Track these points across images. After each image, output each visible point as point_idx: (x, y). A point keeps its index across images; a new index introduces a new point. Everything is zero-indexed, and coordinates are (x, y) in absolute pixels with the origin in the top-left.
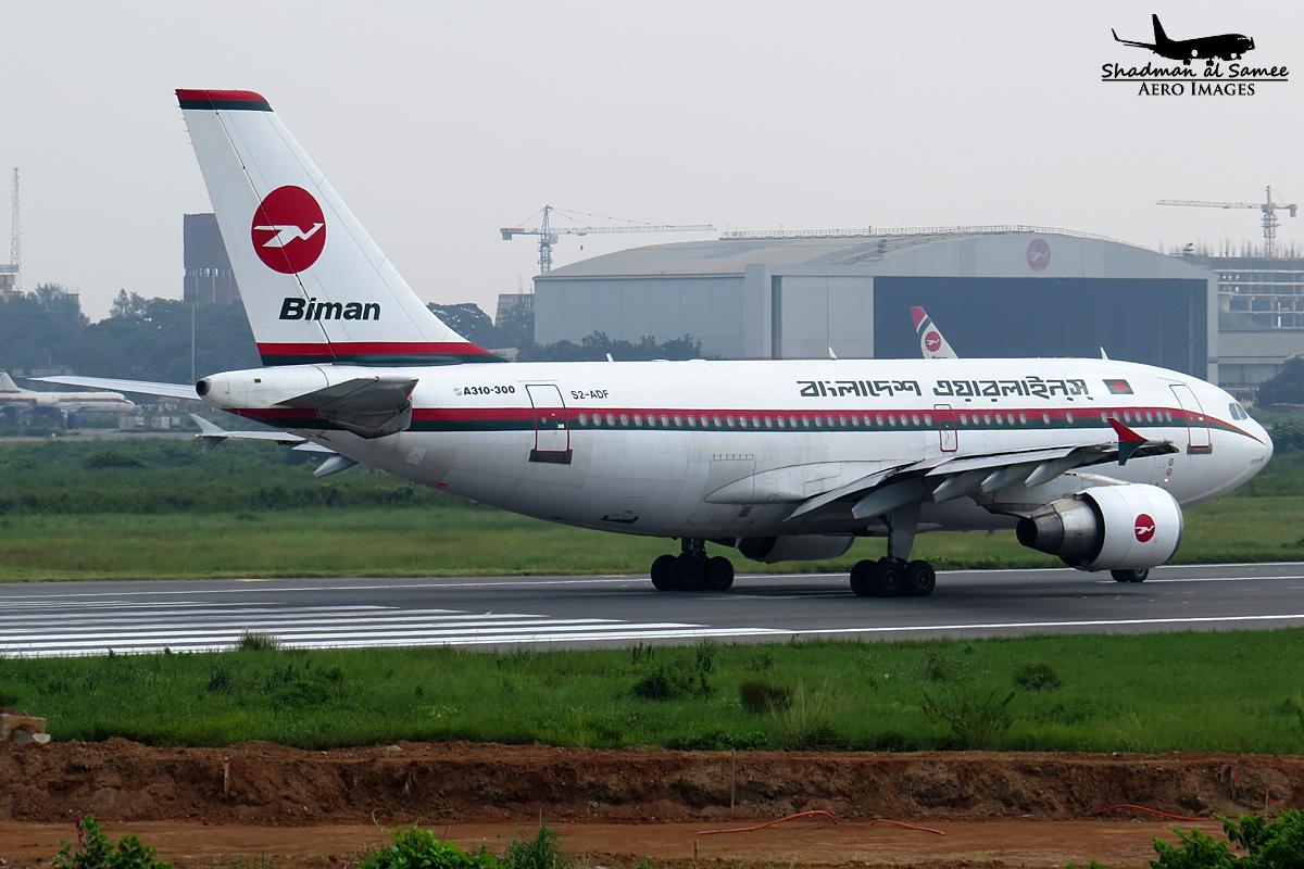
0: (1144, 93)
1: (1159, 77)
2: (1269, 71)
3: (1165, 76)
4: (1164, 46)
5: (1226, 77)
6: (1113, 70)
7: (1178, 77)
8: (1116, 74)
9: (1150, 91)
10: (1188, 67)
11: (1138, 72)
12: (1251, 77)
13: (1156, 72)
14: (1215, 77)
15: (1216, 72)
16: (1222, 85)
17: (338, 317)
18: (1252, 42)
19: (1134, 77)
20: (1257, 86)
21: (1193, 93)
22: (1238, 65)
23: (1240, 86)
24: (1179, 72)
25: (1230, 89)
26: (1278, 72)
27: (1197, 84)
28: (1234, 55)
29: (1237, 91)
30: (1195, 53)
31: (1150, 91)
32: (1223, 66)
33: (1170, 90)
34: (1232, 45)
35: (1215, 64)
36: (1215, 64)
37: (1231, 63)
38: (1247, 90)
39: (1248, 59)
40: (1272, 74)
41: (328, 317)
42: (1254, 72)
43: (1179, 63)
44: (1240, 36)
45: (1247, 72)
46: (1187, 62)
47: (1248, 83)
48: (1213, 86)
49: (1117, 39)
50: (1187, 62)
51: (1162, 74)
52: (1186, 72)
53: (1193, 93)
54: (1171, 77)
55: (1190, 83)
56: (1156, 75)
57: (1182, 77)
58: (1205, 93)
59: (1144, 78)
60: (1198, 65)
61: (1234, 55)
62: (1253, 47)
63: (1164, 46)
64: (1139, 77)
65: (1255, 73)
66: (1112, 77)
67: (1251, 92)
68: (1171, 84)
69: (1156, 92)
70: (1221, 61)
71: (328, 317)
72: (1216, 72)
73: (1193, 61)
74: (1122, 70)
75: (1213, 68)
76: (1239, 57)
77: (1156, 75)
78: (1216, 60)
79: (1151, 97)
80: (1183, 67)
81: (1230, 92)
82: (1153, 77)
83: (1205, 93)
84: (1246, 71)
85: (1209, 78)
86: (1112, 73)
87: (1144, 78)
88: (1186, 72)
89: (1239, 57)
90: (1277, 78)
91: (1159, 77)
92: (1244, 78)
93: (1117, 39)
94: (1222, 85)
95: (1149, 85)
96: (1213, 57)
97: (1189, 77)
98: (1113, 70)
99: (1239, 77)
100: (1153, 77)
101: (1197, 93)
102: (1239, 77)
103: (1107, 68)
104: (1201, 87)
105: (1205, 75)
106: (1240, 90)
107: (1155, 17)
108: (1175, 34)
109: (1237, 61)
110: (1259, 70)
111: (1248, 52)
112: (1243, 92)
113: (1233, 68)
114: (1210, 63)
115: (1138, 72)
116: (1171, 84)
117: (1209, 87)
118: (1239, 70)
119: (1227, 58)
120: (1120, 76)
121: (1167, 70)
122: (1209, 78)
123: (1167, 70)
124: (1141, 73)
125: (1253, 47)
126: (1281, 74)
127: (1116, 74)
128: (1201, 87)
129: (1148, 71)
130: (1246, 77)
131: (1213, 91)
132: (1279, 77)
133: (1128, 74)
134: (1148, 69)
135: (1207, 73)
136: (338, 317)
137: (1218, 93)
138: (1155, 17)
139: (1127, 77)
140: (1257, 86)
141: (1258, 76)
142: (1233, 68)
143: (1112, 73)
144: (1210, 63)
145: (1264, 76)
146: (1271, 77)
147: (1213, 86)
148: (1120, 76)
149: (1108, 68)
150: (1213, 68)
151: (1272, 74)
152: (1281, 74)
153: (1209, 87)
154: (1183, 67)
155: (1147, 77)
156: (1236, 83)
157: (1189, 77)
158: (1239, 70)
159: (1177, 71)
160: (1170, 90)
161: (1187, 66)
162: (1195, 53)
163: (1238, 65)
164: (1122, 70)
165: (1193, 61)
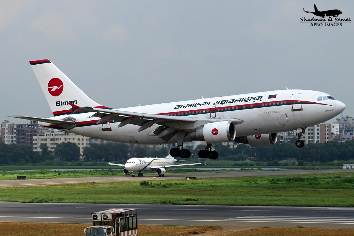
0: (312, 25)
1: (316, 21)
2: (346, 20)
3: (318, 21)
4: (317, 13)
5: (334, 21)
6: (303, 19)
7: (321, 21)
8: (304, 21)
9: (313, 25)
10: (324, 19)
12: (341, 21)
13: (315, 20)
14: (331, 21)
15: (331, 20)
16: (333, 23)
17: (67, 104)
18: (341, 12)
19: (309, 21)
20: (342, 24)
21: (325, 26)
22: (337, 18)
23: (338, 24)
24: (321, 20)
25: (335, 25)
26: (348, 20)
27: (326, 23)
28: (336, 15)
30: (325, 15)
31: (313, 25)
32: (333, 18)
33: (319, 25)
34: (335, 13)
35: (331, 18)
36: (331, 18)
38: (340, 25)
39: (340, 16)
40: (347, 20)
41: (65, 104)
42: (342, 20)
43: (321, 17)
46: (323, 17)
48: (331, 24)
49: (304, 11)
50: (323, 17)
51: (317, 20)
52: (323, 20)
53: (325, 26)
54: (319, 21)
55: (324, 23)
56: (315, 21)
57: (322, 21)
58: (328, 25)
60: (326, 18)
61: (336, 15)
62: (341, 13)
63: (317, 13)
64: (310, 21)
65: (342, 20)
66: (303, 21)
67: (341, 25)
68: (319, 23)
69: (315, 25)
70: (333, 17)
71: (65, 104)
72: (331, 20)
73: (325, 17)
74: (306, 19)
75: (331, 19)
76: (337, 16)
77: (315, 21)
78: (331, 17)
79: (314, 27)
80: (322, 19)
81: (335, 25)
82: (314, 21)
83: (328, 25)
84: (339, 20)
85: (329, 21)
86: (303, 20)
87: (312, 21)
88: (323, 20)
89: (337, 16)
91: (316, 21)
92: (339, 21)
93: (304, 11)
94: (333, 23)
95: (313, 23)
97: (324, 21)
98: (303, 19)
99: (338, 21)
100: (314, 21)
101: (326, 25)
102: (338, 21)
104: (327, 24)
105: (328, 21)
106: (338, 25)
107: (315, 5)
108: (320, 10)
109: (337, 17)
110: (343, 19)
111: (340, 14)
112: (339, 25)
113: (336, 19)
114: (330, 17)
117: (329, 24)
118: (338, 19)
119: (334, 16)
120: (305, 21)
121: (318, 19)
122: (329, 21)
123: (318, 19)
124: (311, 20)
125: (341, 13)
126: (349, 20)
127: (304, 21)
128: (327, 24)
129: (313, 20)
130: (340, 21)
131: (330, 25)
132: (348, 21)
133: (308, 20)
134: (313, 19)
135: (329, 20)
136: (67, 104)
137: (332, 26)
138: (315, 5)
139: (307, 21)
140: (342, 24)
141: (343, 21)
142: (336, 19)
143: (303, 20)
144: (330, 17)
145: (344, 21)
146: (346, 21)
147: (331, 24)
148: (305, 21)
150: (331, 19)
151: (347, 20)
152: (349, 20)
153: (329, 24)
154: (322, 19)
155: (313, 21)
156: (337, 23)
157: (324, 21)
158: (338, 19)
159: (321, 20)
160: (319, 25)
161: (323, 18)
162: (325, 15)
163: (337, 18)
164: (306, 19)
165: (325, 17)
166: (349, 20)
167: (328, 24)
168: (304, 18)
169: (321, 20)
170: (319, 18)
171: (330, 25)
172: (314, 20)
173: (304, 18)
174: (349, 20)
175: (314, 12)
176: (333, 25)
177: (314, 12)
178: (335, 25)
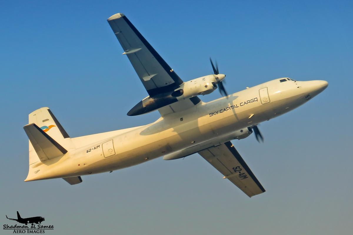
0: (15, 232)
1: (19, 228)
2: (48, 227)
3: (20, 228)
4: (20, 220)
5: (37, 228)
6: (6, 226)
7: (24, 228)
8: (7, 228)
9: (16, 232)
10: (27, 226)
11: (13, 227)
13: (18, 227)
14: (34, 228)
15: (34, 227)
16: (36, 230)
18: (44, 219)
19: (12, 228)
20: (45, 231)
21: (28, 233)
22: (40, 225)
23: (41, 231)
24: (24, 227)
25: (38, 232)
26: (51, 227)
27: (29, 230)
28: (39, 222)
29: (40, 232)
30: (28, 222)
31: (16, 232)
32: (36, 225)
33: (22, 232)
34: (38, 220)
35: (34, 225)
36: (34, 225)
37: (38, 224)
38: (43, 232)
39: (43, 223)
40: (49, 227)
43: (24, 224)
44: (41, 217)
45: (43, 227)
46: (26, 224)
47: (43, 230)
48: (33, 231)
49: (7, 218)
50: (26, 224)
52: (26, 227)
53: (28, 233)
54: (22, 228)
55: (27, 230)
57: (25, 228)
58: (31, 232)
59: (15, 228)
60: (29, 225)
61: (39, 222)
62: (44, 220)
63: (20, 220)
64: (13, 228)
66: (6, 228)
67: (44, 232)
68: (22, 230)
69: (18, 232)
70: (35, 224)
72: (34, 227)
73: (28, 224)
74: (9, 226)
75: (33, 226)
76: (40, 223)
78: (34, 224)
79: (17, 234)
80: (25, 226)
81: (38, 232)
82: (17, 228)
83: (31, 232)
84: (42, 227)
85: (32, 228)
86: (6, 227)
87: (15, 228)
88: (26, 227)
89: (40, 223)
90: (51, 228)
91: (19, 228)
92: (42, 228)
93: (7, 218)
94: (36, 230)
95: (16, 230)
96: (33, 223)
97: (27, 228)
98: (6, 226)
99: (40, 228)
100: (17, 228)
101: (29, 232)
102: (40, 228)
103: (5, 226)
104: (30, 231)
106: (41, 231)
107: (18, 212)
108: (23, 217)
109: (40, 224)
110: (46, 226)
111: (43, 221)
112: (41, 232)
113: (39, 226)
114: (33, 224)
115: (13, 227)
116: (22, 230)
118: (41, 226)
119: (37, 223)
120: (8, 228)
121: (21, 226)
122: (32, 228)
123: (21, 226)
124: (14, 227)
126: (52, 227)
127: (7, 228)
128: (30, 231)
129: (16, 227)
131: (33, 232)
132: (51, 228)
133: (10, 227)
134: (16, 226)
135: (32, 227)
137: (35, 233)
138: (18, 212)
139: (10, 228)
140: (45, 231)
141: (45, 228)
142: (39, 226)
143: (6, 227)
144: (33, 224)
145: (47, 228)
146: (49, 228)
147: (33, 231)
148: (8, 228)
149: (5, 226)
150: (33, 226)
151: (49, 227)
152: (52, 227)
153: (32, 231)
154: (25, 226)
155: (16, 228)
156: (40, 230)
157: (27, 228)
158: (41, 226)
159: (24, 227)
160: (22, 232)
161: (26, 225)
162: (28, 222)
163: (40, 225)
164: (9, 226)
166: (51, 227)
167: (31, 231)
168: (7, 225)
169: (24, 227)
170: (22, 225)
171: (33, 232)
172: (17, 226)
173: (7, 225)
174: (51, 227)
175: (17, 219)
176: (36, 232)
177: (17, 219)
178: (38, 232)
